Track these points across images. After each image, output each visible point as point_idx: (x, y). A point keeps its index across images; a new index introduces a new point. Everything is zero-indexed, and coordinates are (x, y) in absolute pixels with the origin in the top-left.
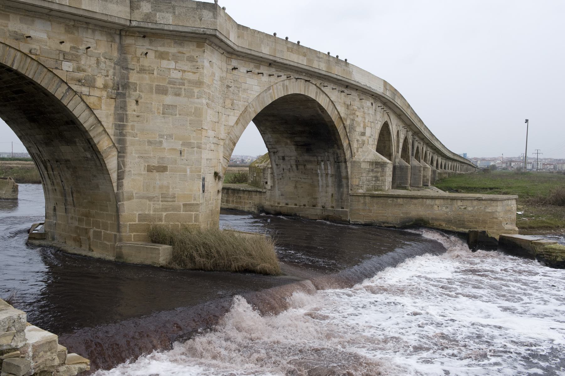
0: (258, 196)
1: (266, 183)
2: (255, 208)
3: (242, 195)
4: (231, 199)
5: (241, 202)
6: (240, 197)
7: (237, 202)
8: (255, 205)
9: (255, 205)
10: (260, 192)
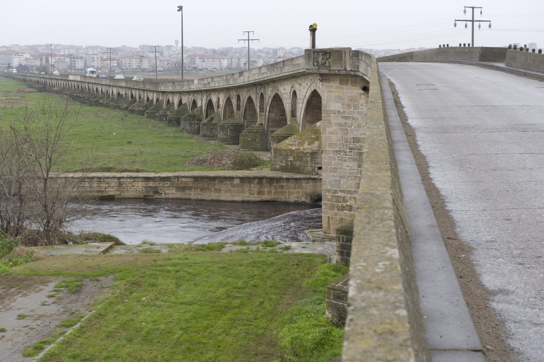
0: (311, 183)
1: (320, 168)
2: (307, 198)
3: (285, 184)
4: (266, 190)
5: (282, 193)
6: (282, 187)
7: (276, 193)
8: (306, 194)
9: (306, 194)
10: (315, 179)
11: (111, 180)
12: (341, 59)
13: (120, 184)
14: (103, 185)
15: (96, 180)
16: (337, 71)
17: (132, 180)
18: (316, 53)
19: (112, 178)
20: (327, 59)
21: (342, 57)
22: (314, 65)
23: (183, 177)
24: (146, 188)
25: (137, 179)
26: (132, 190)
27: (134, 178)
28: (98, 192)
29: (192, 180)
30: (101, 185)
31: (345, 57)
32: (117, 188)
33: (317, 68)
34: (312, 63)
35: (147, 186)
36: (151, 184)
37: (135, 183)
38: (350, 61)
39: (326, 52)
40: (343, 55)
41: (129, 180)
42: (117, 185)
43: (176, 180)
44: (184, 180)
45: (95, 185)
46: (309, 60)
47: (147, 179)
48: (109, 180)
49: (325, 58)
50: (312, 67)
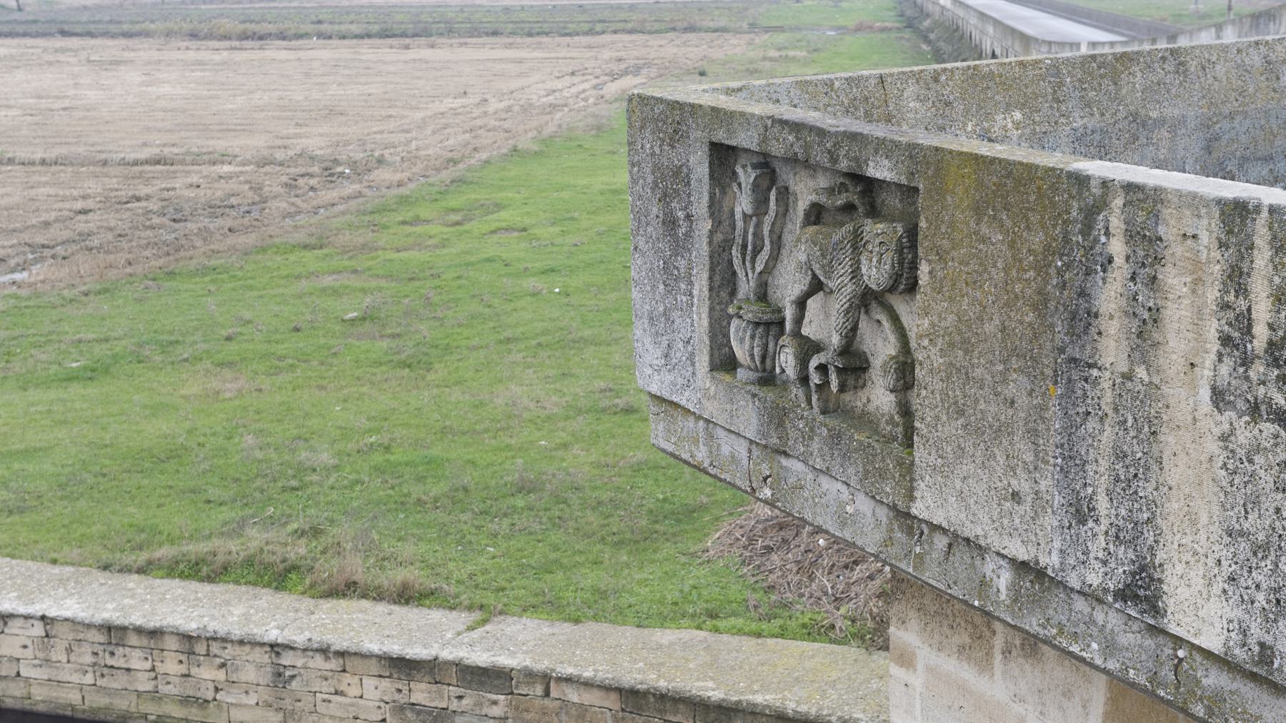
11: (238, 650)
12: (1079, 367)
13: (280, 678)
14: (207, 673)
15: (171, 643)
16: (1004, 580)
17: (334, 664)
18: (746, 176)
19: (241, 642)
20: (866, 300)
21: (1083, 320)
22: (725, 363)
23: (569, 680)
24: (400, 709)
25: (357, 661)
26: (333, 709)
27: (342, 654)
28: (186, 701)
29: (612, 702)
30: (194, 671)
31: (1146, 329)
32: (265, 694)
33: (749, 418)
34: (701, 320)
35: (403, 699)
36: (421, 693)
37: (347, 678)
38: (1238, 464)
39: (869, 186)
40: (1110, 295)
41: (318, 661)
42: (266, 677)
43: (539, 690)
44: (573, 695)
45: (171, 666)
46: (671, 277)
47: (402, 667)
48: (230, 651)
49: (843, 289)
50: (700, 388)
